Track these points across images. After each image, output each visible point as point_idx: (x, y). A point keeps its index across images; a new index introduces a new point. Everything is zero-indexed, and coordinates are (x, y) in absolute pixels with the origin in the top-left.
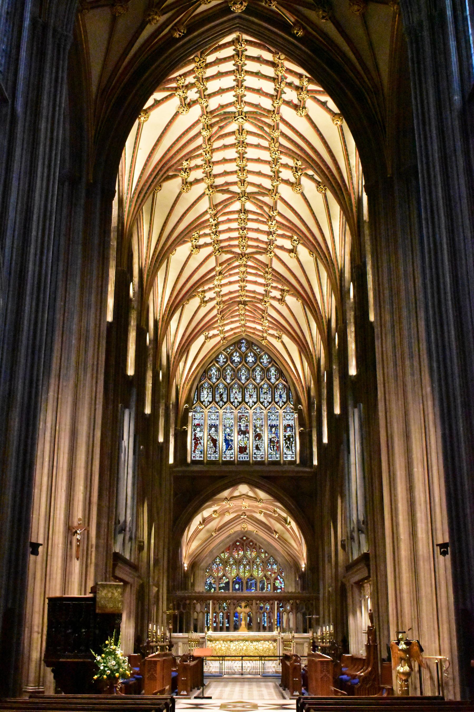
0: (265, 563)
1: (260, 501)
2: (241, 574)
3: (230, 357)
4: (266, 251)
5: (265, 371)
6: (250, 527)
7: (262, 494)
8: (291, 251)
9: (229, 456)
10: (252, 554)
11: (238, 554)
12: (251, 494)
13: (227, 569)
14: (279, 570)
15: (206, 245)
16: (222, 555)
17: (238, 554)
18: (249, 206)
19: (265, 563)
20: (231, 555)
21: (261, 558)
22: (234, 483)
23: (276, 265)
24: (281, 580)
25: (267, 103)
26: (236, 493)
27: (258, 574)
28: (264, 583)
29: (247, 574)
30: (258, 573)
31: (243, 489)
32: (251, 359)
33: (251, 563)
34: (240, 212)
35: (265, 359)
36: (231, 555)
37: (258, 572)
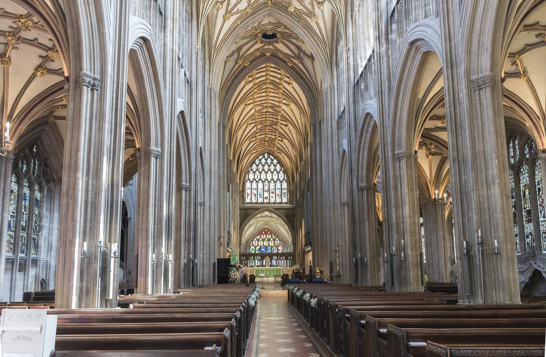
0: (274, 240)
1: (273, 218)
3: (260, 160)
4: (276, 125)
5: (275, 166)
6: (269, 227)
7: (274, 215)
8: (286, 126)
9: (260, 200)
10: (269, 237)
12: (270, 215)
15: (252, 123)
18: (270, 110)
19: (274, 240)
20: (261, 237)
22: (263, 211)
23: (280, 130)
25: (278, 81)
26: (264, 215)
30: (271, 244)
31: (267, 213)
32: (269, 161)
33: (269, 240)
34: (266, 112)
35: (275, 161)
36: (261, 237)
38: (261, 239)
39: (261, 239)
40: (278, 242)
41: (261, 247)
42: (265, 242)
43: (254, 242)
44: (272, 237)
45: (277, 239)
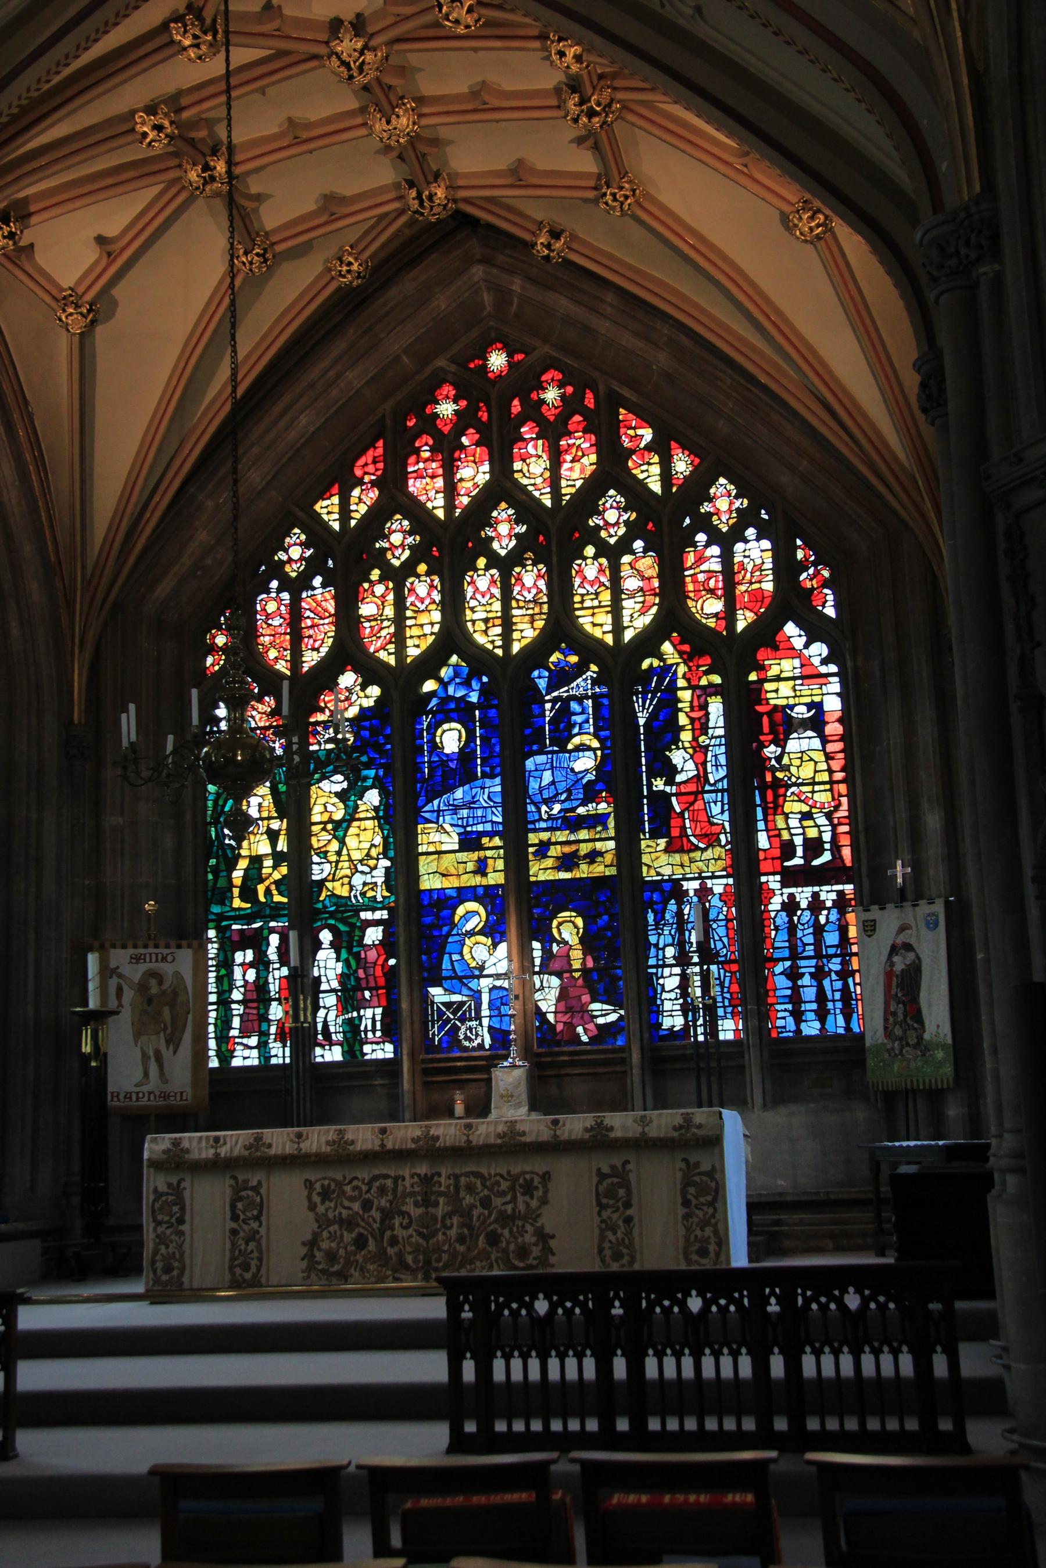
0: (668, 525)
2: (487, 638)
11: (451, 490)
13: (367, 609)
14: (786, 568)
16: (328, 509)
17: (451, 490)
19: (668, 525)
21: (635, 494)
24: (819, 650)
27: (618, 628)
28: (673, 688)
29: (526, 634)
37: (616, 609)
38: (398, 539)
39: (398, 539)
40: (755, 552)
41: (400, 683)
42: (482, 582)
43: (272, 605)
44: (612, 471)
45: (724, 501)
